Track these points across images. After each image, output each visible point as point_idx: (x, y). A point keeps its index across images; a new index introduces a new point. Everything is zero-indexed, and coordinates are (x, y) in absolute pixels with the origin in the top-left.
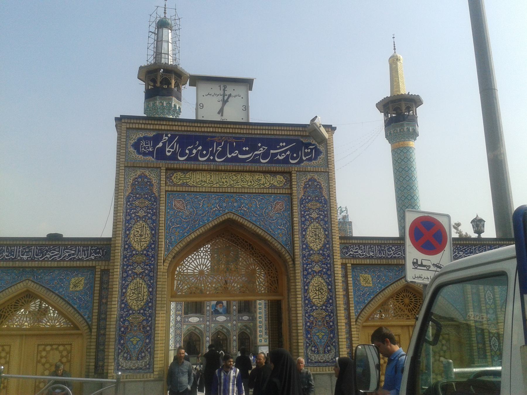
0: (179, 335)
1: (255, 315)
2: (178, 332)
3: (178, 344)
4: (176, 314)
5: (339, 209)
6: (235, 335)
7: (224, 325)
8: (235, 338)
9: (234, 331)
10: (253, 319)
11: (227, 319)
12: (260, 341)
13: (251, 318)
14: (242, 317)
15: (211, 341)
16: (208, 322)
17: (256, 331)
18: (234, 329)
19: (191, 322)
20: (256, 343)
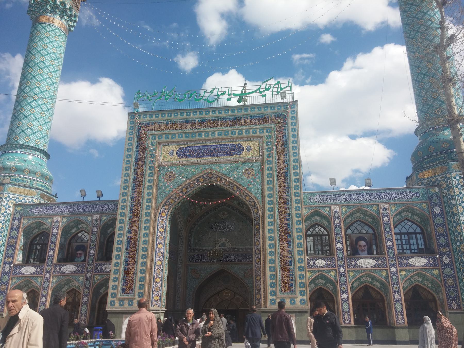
5: (277, 86)
6: (87, 295)
8: (86, 299)
9: (86, 288)
11: (77, 270)
12: (111, 305)
14: (102, 266)
16: (48, 274)
18: (87, 286)
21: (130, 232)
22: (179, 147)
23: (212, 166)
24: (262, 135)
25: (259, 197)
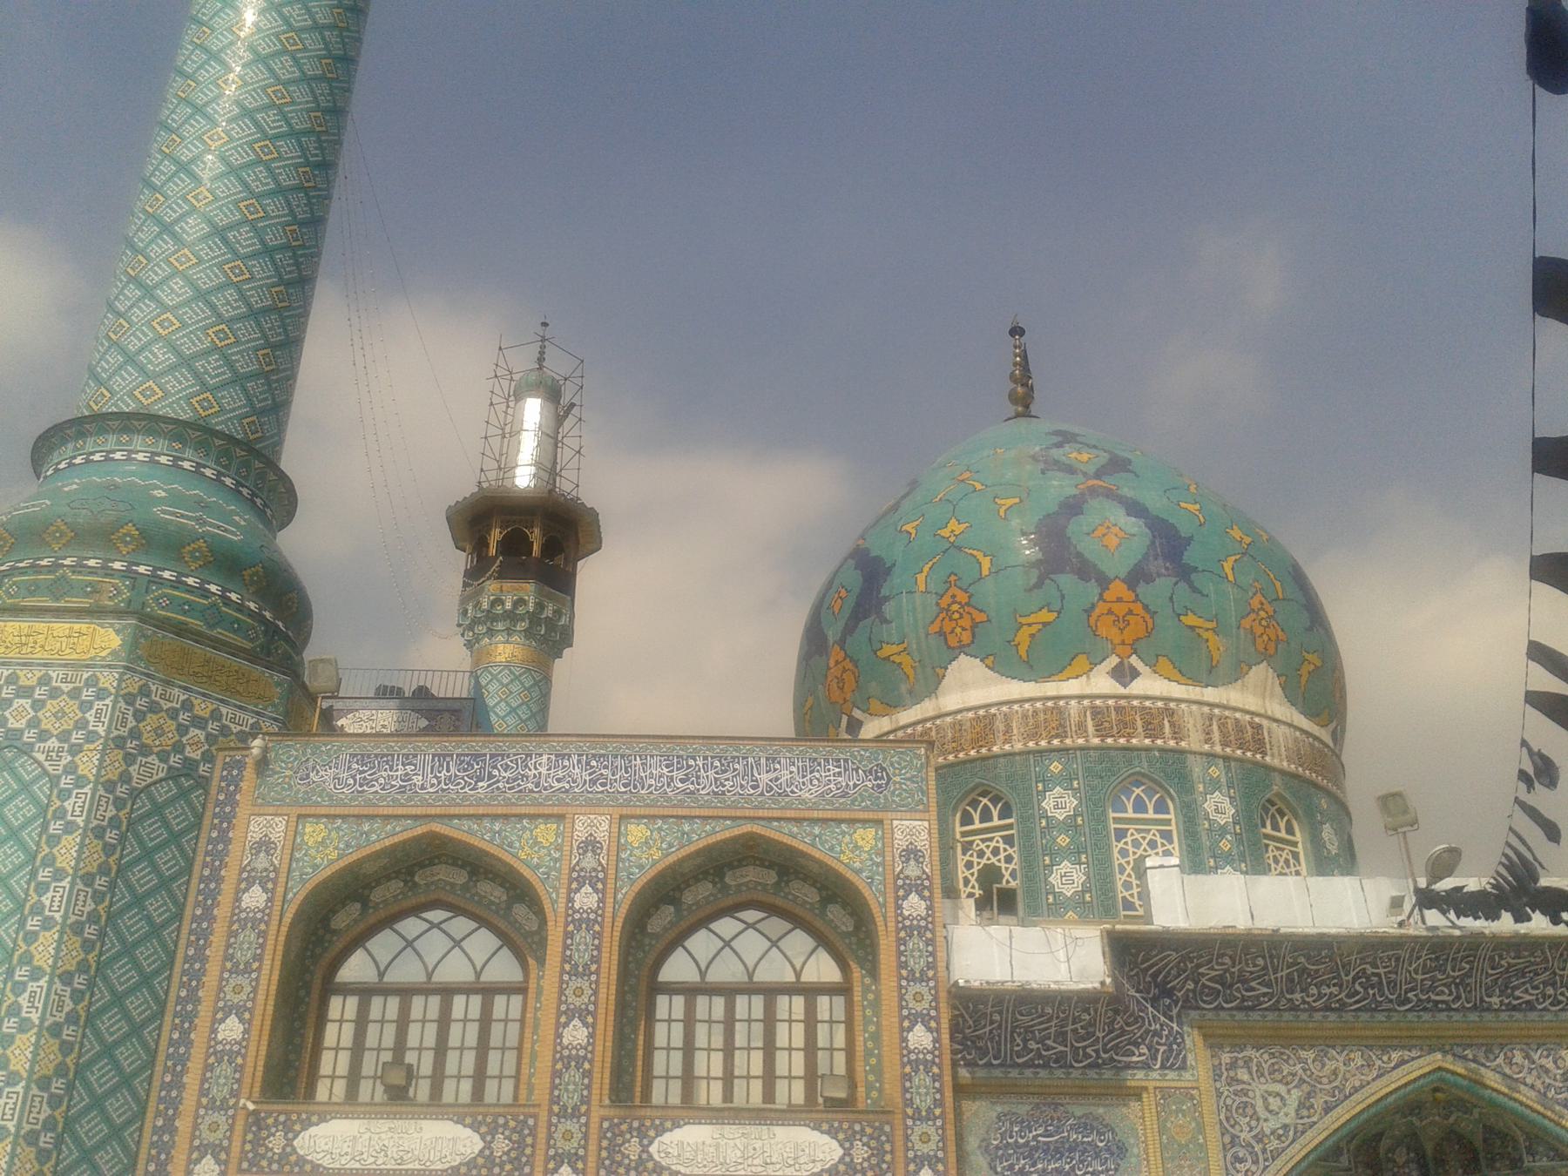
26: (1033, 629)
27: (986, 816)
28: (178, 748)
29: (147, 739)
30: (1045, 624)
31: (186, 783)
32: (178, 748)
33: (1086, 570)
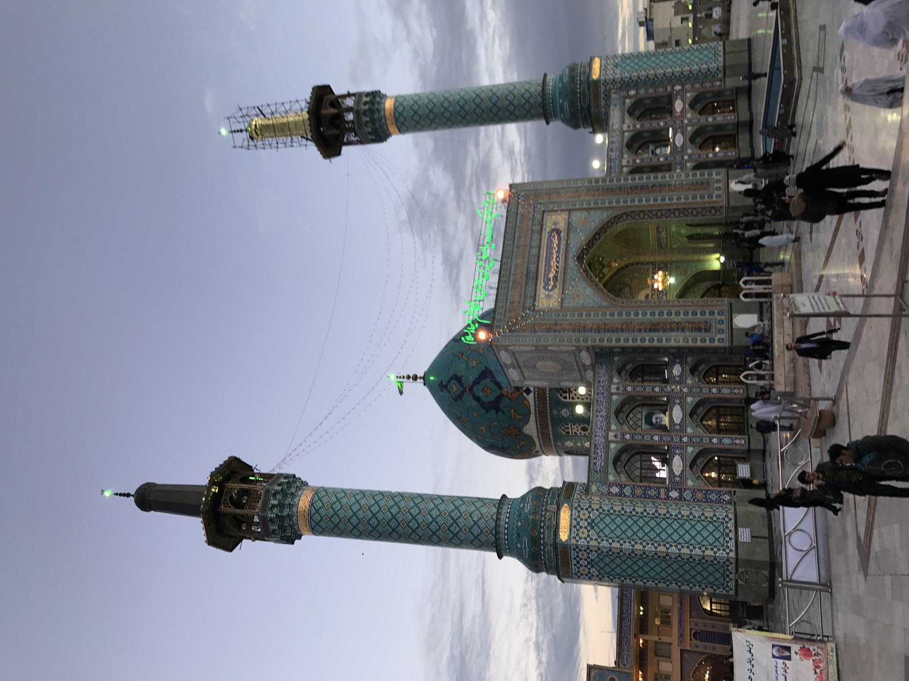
0: (705, 494)
1: (673, 350)
2: (700, 496)
3: (724, 497)
4: (665, 499)
7: (689, 410)
10: (678, 354)
11: (679, 404)
13: (678, 360)
15: (719, 436)
17: (703, 350)
19: (683, 471)
20: (725, 348)
21: (640, 330)
22: (543, 290)
23: (571, 255)
24: (541, 212)
25: (610, 212)
26: (516, 415)
27: (568, 428)
28: (586, 528)
29: (585, 535)
30: (515, 411)
31: (593, 524)
32: (586, 528)
33: (499, 398)
